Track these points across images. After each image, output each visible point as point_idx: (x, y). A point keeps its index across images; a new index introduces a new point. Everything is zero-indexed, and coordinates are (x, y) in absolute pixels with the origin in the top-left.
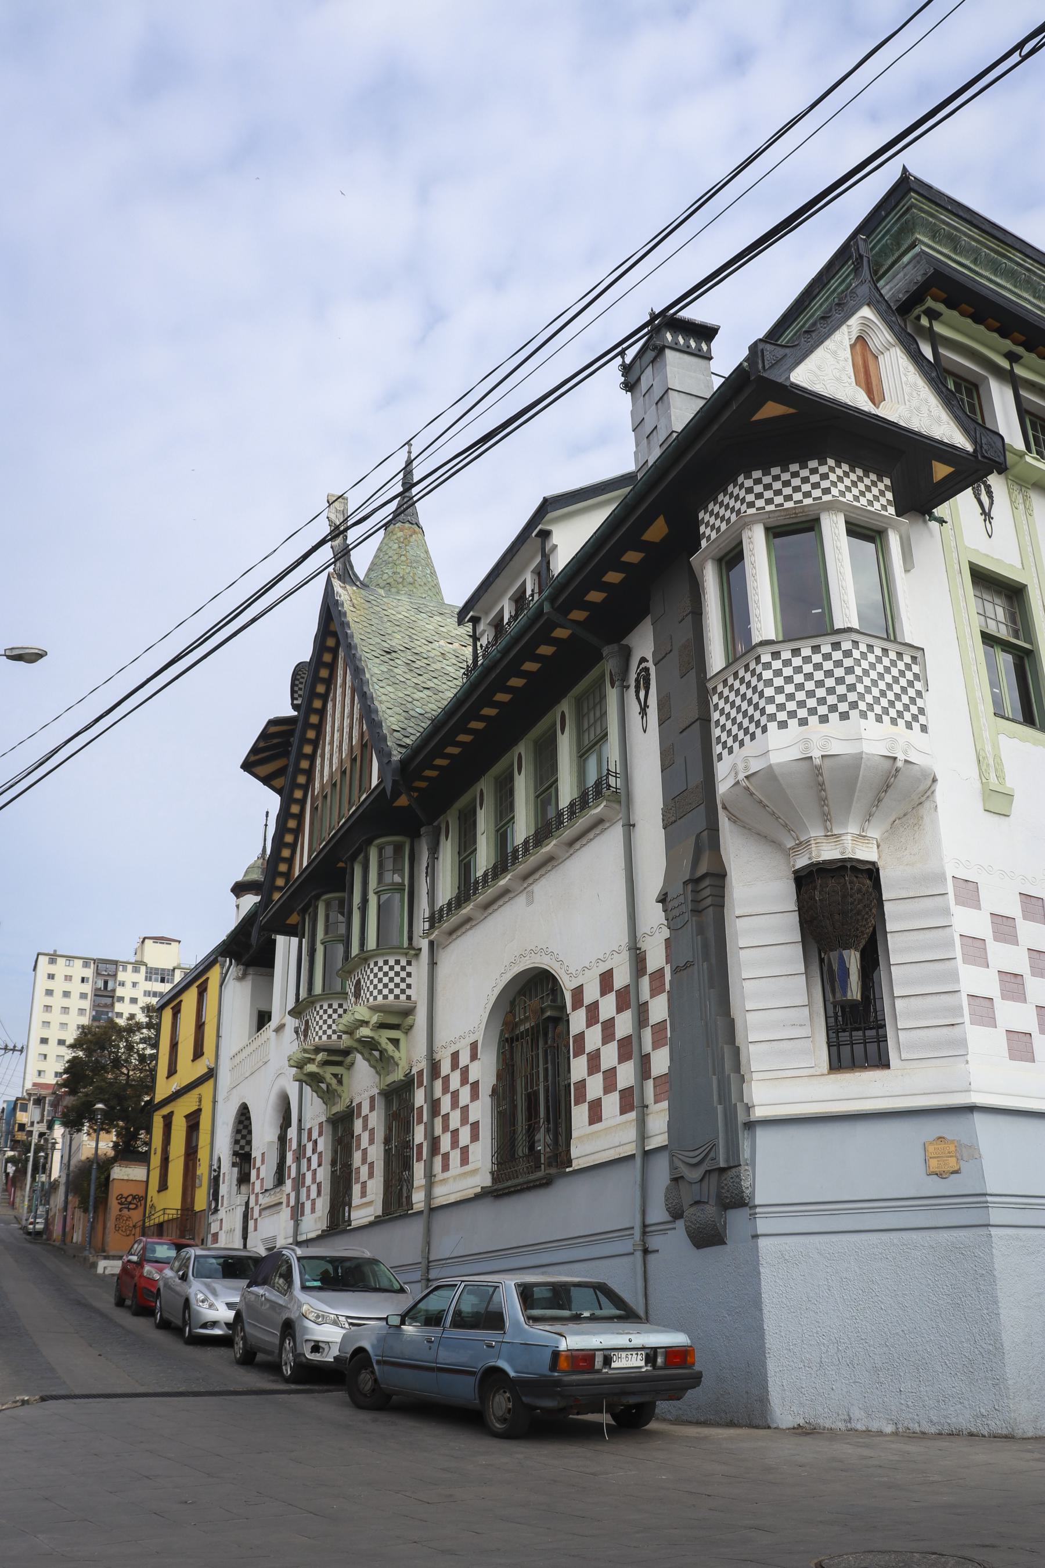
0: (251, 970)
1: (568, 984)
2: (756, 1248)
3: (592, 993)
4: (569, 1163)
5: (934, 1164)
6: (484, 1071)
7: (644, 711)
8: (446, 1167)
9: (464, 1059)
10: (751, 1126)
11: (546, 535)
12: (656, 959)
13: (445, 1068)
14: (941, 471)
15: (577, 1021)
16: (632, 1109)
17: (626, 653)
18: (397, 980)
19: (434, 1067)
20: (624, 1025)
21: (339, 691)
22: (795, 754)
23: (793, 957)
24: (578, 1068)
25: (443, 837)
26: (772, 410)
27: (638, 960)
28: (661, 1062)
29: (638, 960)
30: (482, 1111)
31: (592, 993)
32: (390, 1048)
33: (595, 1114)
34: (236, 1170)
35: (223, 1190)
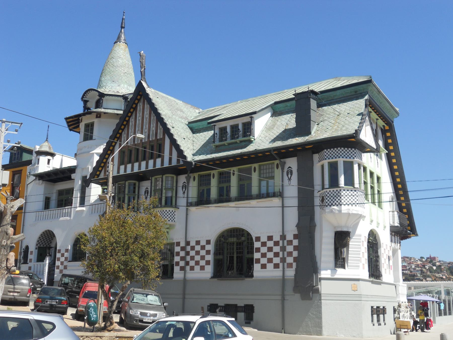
0: (44, 182)
1: (254, 236)
2: (321, 303)
3: (264, 239)
4: (252, 276)
5: (353, 289)
6: (210, 247)
7: (290, 179)
8: (192, 268)
9: (203, 243)
10: (321, 279)
11: (251, 117)
12: (290, 237)
13: (193, 243)
14: (369, 150)
15: (257, 245)
16: (278, 268)
17: (285, 163)
18: (168, 214)
19: (188, 243)
20: (276, 249)
21: (139, 118)
22: (346, 212)
23: (332, 247)
24: (257, 256)
25: (192, 180)
26: (353, 140)
27: (283, 237)
28: (290, 260)
29: (283, 237)
30: (210, 258)
31: (264, 239)
32: (167, 234)
33: (264, 266)
34: (37, 250)
35: (30, 257)
